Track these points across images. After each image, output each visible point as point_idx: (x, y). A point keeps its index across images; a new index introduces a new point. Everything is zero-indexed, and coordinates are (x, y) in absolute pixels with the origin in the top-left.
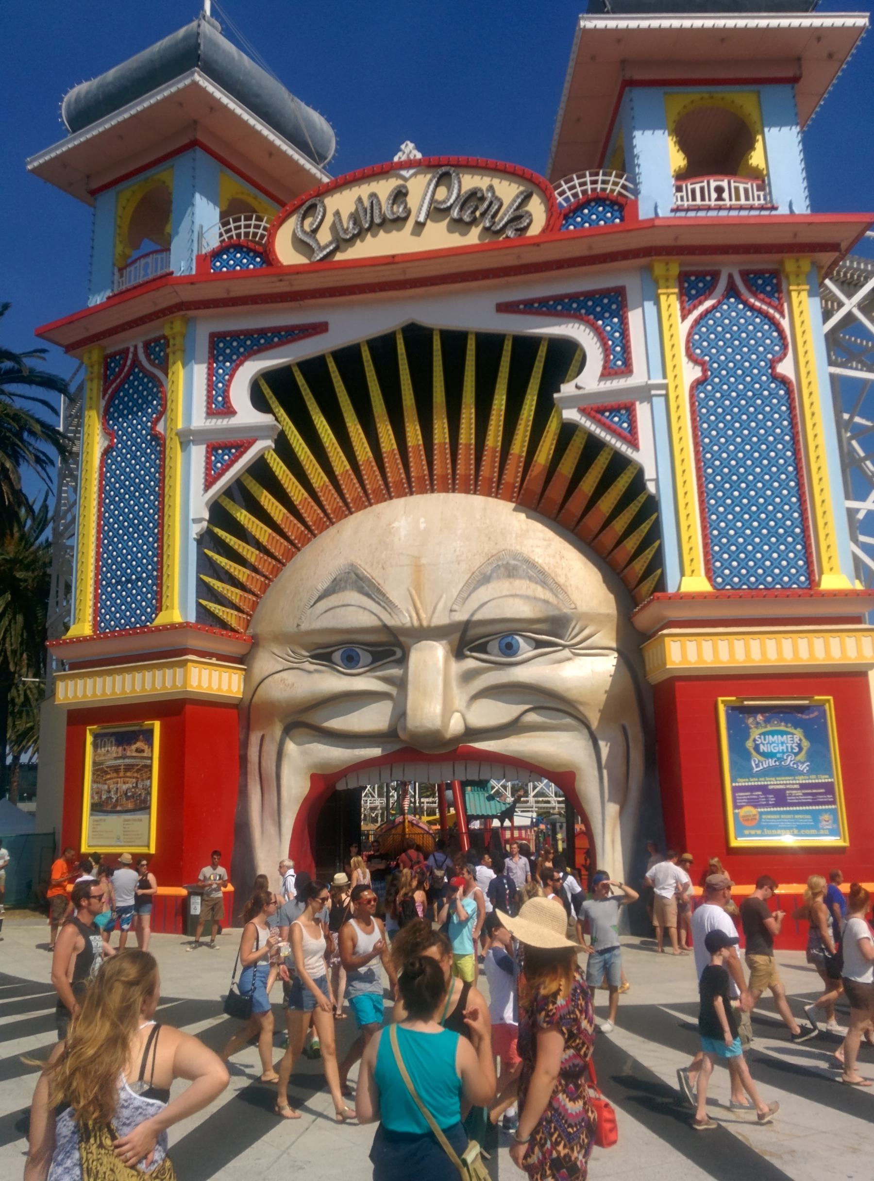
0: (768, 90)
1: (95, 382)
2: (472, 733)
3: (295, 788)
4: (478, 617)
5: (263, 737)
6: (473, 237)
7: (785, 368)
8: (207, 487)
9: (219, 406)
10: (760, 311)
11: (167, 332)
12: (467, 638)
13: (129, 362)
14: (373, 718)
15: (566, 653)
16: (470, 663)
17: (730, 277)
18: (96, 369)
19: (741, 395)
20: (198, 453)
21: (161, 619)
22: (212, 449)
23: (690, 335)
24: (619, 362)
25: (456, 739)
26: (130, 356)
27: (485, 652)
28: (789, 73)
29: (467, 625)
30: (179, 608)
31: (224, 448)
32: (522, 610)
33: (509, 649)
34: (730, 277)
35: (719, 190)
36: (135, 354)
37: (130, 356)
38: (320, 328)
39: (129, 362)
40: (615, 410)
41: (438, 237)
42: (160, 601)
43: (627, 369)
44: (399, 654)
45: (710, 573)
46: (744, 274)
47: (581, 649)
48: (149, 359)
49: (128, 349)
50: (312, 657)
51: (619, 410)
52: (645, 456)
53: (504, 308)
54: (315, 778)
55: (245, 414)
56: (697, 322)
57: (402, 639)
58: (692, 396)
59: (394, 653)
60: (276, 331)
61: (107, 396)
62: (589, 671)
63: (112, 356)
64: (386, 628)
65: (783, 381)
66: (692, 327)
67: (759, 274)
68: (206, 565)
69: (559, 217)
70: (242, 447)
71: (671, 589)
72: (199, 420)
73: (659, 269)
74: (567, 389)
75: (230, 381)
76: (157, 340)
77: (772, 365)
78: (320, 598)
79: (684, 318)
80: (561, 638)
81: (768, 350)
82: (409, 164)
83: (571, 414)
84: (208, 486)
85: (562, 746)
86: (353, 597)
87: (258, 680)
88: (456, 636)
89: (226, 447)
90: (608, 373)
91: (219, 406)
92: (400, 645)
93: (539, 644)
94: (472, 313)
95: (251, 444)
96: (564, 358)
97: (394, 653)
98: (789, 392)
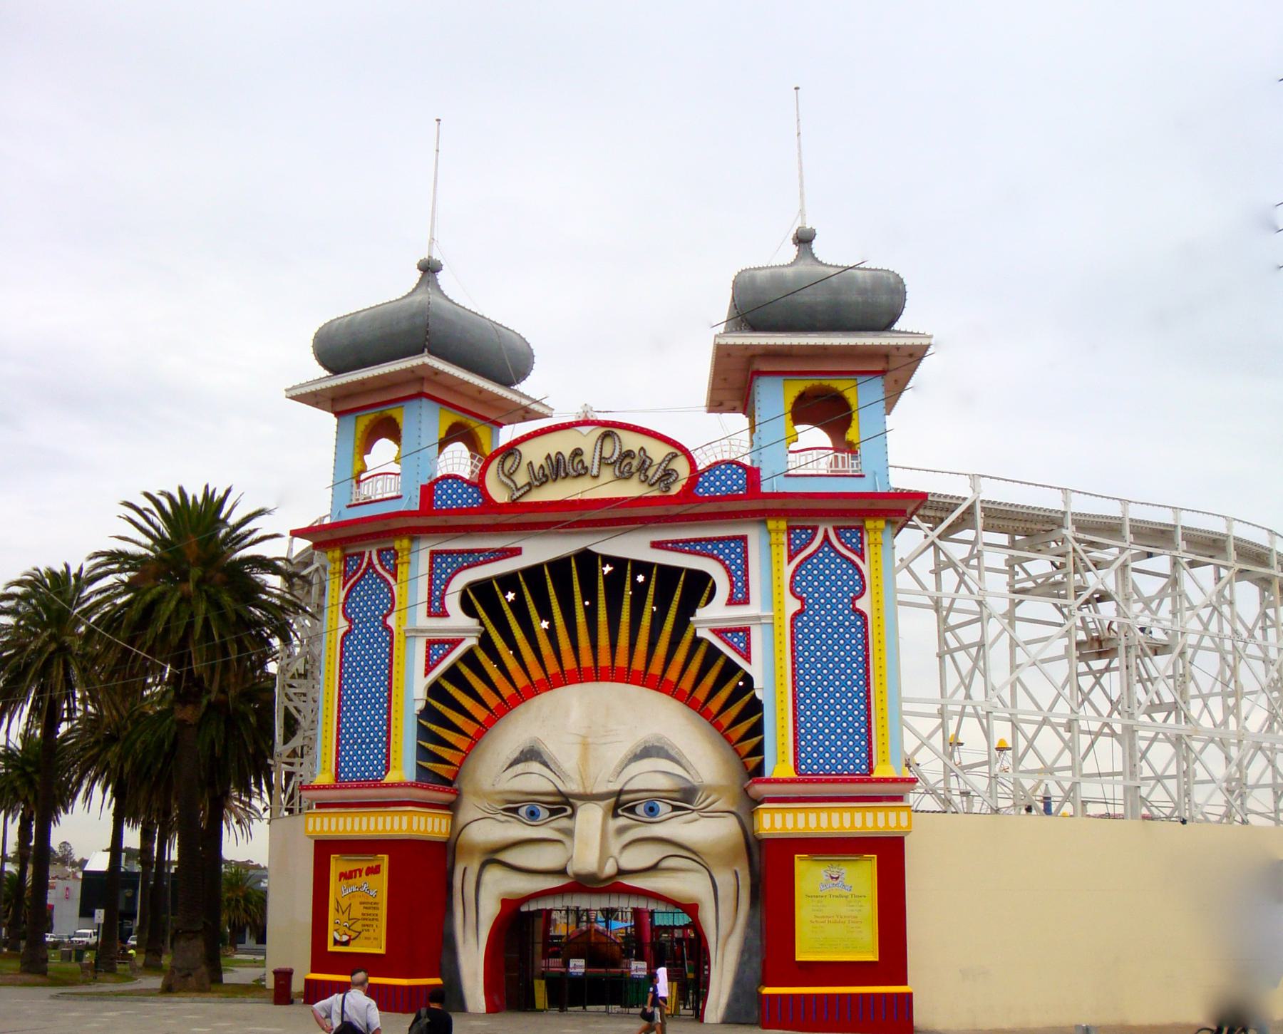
0: (861, 379)
2: (621, 872)
3: (490, 910)
4: (627, 788)
6: (633, 489)
7: (862, 604)
8: (427, 674)
9: (437, 610)
10: (848, 559)
11: (397, 545)
13: (364, 565)
14: (547, 858)
15: (695, 815)
16: (622, 821)
17: (826, 531)
19: (829, 625)
20: (420, 648)
21: (391, 777)
22: (430, 643)
23: (793, 577)
24: (739, 597)
25: (610, 878)
26: (366, 560)
27: (634, 813)
28: (878, 367)
29: (621, 792)
30: (403, 768)
32: (663, 783)
33: (652, 810)
34: (826, 531)
36: (370, 558)
37: (366, 560)
38: (516, 552)
39: (364, 565)
40: (735, 631)
41: (607, 488)
42: (388, 762)
43: (746, 601)
44: (569, 811)
46: (836, 529)
47: (706, 813)
48: (380, 562)
50: (505, 810)
52: (755, 669)
53: (656, 545)
54: (505, 902)
55: (458, 620)
56: (798, 566)
58: (792, 626)
59: (565, 810)
62: (711, 830)
63: (352, 555)
64: (560, 793)
65: (862, 614)
66: (794, 571)
67: (849, 528)
68: (423, 733)
70: (455, 643)
71: (769, 772)
73: (772, 524)
74: (702, 613)
76: (388, 550)
77: (854, 600)
78: (511, 765)
79: (789, 562)
81: (852, 589)
83: (703, 633)
84: (427, 674)
86: (535, 766)
88: (613, 800)
89: (442, 642)
90: (731, 601)
91: (437, 610)
93: (675, 808)
94: (634, 546)
96: (699, 587)
98: (865, 624)
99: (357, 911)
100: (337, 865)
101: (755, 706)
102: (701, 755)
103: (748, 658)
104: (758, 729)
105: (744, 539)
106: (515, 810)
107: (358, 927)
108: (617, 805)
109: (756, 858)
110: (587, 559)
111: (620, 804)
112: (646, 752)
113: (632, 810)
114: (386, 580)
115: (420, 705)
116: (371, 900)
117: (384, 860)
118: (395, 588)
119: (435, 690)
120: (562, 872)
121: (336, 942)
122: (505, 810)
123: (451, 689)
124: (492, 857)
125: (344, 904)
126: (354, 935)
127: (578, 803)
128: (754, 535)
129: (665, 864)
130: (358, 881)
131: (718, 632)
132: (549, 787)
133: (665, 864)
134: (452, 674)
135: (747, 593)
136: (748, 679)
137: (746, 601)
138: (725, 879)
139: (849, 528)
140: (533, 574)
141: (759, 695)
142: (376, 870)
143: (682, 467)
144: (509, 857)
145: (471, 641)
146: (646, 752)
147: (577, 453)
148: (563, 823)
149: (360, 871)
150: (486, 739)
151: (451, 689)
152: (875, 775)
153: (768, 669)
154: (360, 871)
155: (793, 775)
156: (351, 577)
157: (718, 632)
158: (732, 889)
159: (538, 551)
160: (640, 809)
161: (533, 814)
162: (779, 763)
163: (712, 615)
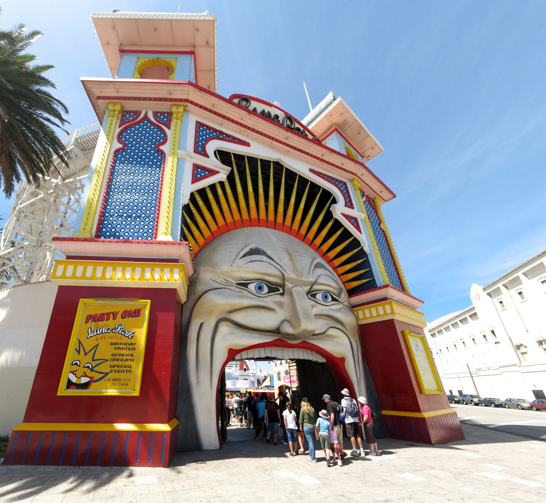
1: (115, 119)
5: (202, 324)
12: (312, 290)
14: (268, 320)
18: (117, 113)
31: (199, 172)
38: (247, 144)
48: (156, 120)
49: (141, 112)
53: (311, 171)
55: (213, 162)
57: (286, 283)
59: (279, 290)
60: (228, 136)
61: (121, 128)
70: (212, 172)
80: (340, 298)
87: (200, 293)
92: (283, 286)
93: (334, 299)
97: (279, 290)
100: (86, 307)
101: (362, 254)
104: (366, 264)
106: (246, 285)
107: (105, 368)
110: (278, 166)
114: (160, 127)
116: (125, 340)
122: (237, 284)
125: (88, 345)
130: (111, 323)
136: (356, 243)
141: (366, 249)
142: (137, 313)
144: (239, 317)
145: (222, 176)
150: (216, 243)
154: (115, 315)
156: (126, 123)
160: (319, 296)
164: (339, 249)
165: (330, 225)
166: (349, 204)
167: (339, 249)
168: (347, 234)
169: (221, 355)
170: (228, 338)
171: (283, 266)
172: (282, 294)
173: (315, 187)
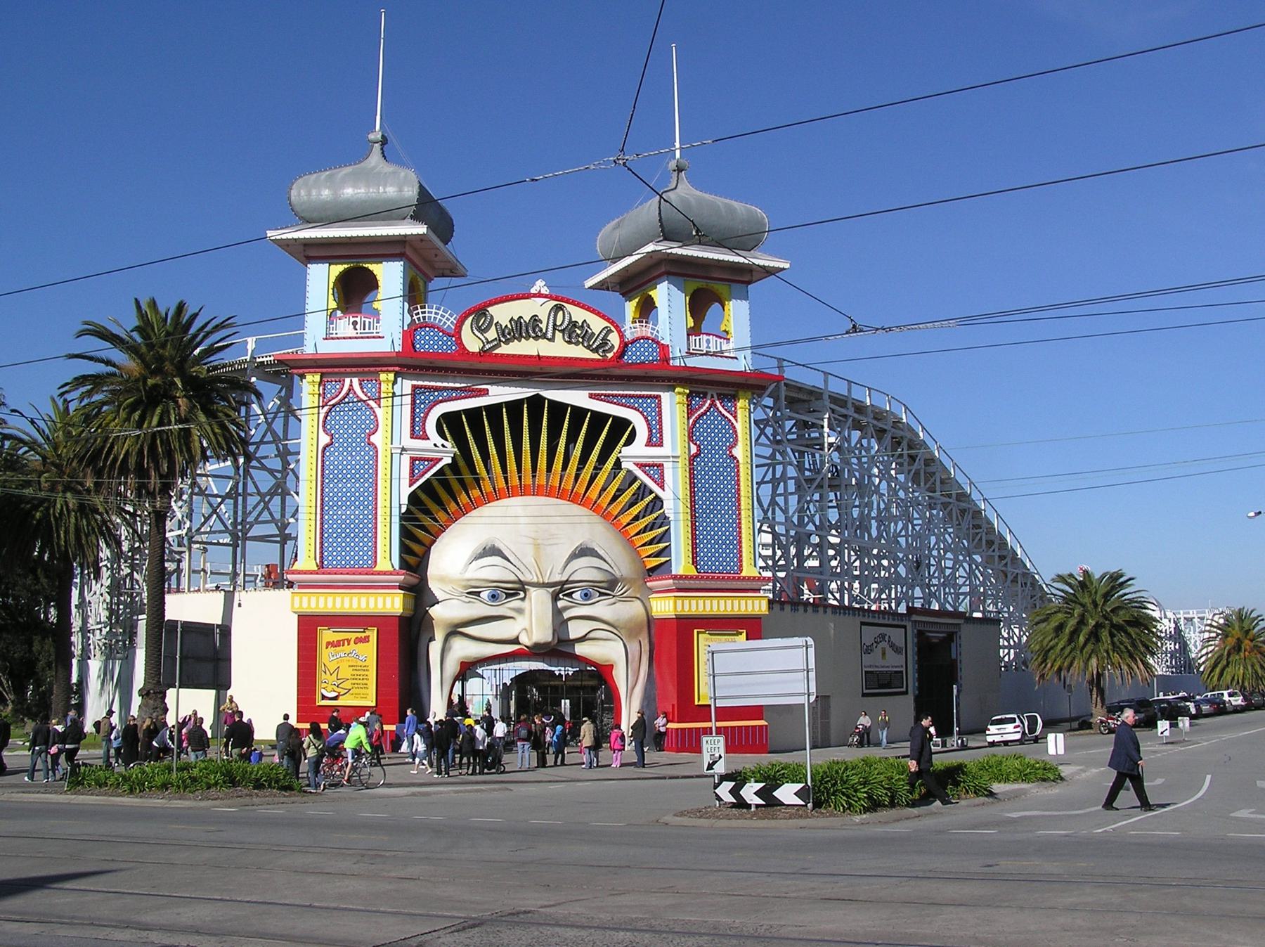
6: (579, 352)
22: (413, 460)
24: (655, 440)
29: (567, 582)
35: (708, 341)
38: (485, 393)
41: (559, 348)
43: (661, 445)
45: (695, 563)
46: (719, 395)
51: (654, 469)
53: (591, 396)
56: (695, 422)
64: (520, 582)
67: (726, 396)
68: (405, 533)
69: (625, 346)
72: (409, 442)
74: (627, 451)
75: (426, 417)
82: (540, 295)
85: (605, 650)
90: (649, 443)
91: (418, 432)
93: (601, 594)
94: (577, 397)
95: (441, 459)
99: (345, 672)
100: (326, 635)
101: (664, 520)
102: (618, 559)
103: (662, 487)
104: (665, 536)
105: (658, 397)
106: (478, 594)
107: (347, 685)
108: (561, 591)
109: (653, 632)
111: (561, 590)
112: (584, 551)
113: (570, 595)
115: (404, 510)
116: (360, 663)
117: (373, 634)
118: (377, 410)
119: (413, 498)
120: (516, 641)
121: (324, 697)
123: (423, 497)
124: (455, 630)
126: (343, 692)
127: (532, 589)
128: (666, 397)
129: (591, 635)
130: (347, 648)
131: (640, 466)
132: (513, 578)
133: (591, 635)
134: (427, 486)
135: (661, 438)
136: (658, 502)
137: (661, 445)
138: (633, 647)
139: (726, 396)
140: (494, 410)
142: (366, 640)
143: (614, 339)
146: (584, 551)
147: (535, 319)
148: (515, 603)
149: (349, 641)
151: (423, 497)
152: (744, 574)
153: (674, 496)
154: (349, 641)
155: (694, 572)
157: (640, 466)
158: (637, 654)
159: (500, 394)
160: (577, 596)
161: (493, 596)
162: (681, 563)
163: (633, 454)
164: (635, 510)
165: (622, 474)
166: (655, 440)
167: (635, 510)
168: (644, 490)
169: (452, 667)
170: (463, 649)
171: (522, 568)
172: (523, 599)
173: (599, 419)
